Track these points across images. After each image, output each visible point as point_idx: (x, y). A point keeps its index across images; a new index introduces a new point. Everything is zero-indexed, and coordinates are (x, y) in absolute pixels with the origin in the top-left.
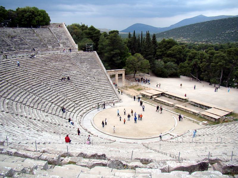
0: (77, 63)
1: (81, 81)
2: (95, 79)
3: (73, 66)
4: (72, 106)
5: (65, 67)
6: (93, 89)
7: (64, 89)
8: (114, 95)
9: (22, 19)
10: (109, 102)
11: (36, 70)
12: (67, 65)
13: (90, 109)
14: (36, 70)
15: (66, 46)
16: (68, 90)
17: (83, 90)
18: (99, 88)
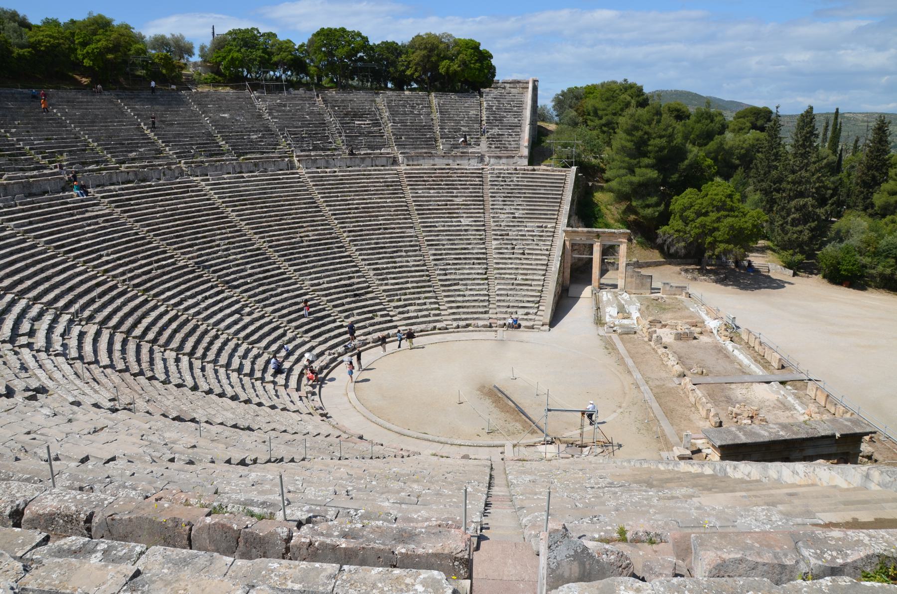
0: (494, 197)
1: (465, 249)
2: (513, 248)
3: (474, 205)
4: (369, 312)
5: (446, 205)
6: (485, 276)
7: (395, 262)
8: (537, 305)
9: (408, 67)
10: (502, 322)
11: (353, 204)
12: (458, 200)
13: (421, 331)
14: (353, 204)
15: (496, 148)
16: (400, 267)
17: (451, 273)
18: (503, 279)
